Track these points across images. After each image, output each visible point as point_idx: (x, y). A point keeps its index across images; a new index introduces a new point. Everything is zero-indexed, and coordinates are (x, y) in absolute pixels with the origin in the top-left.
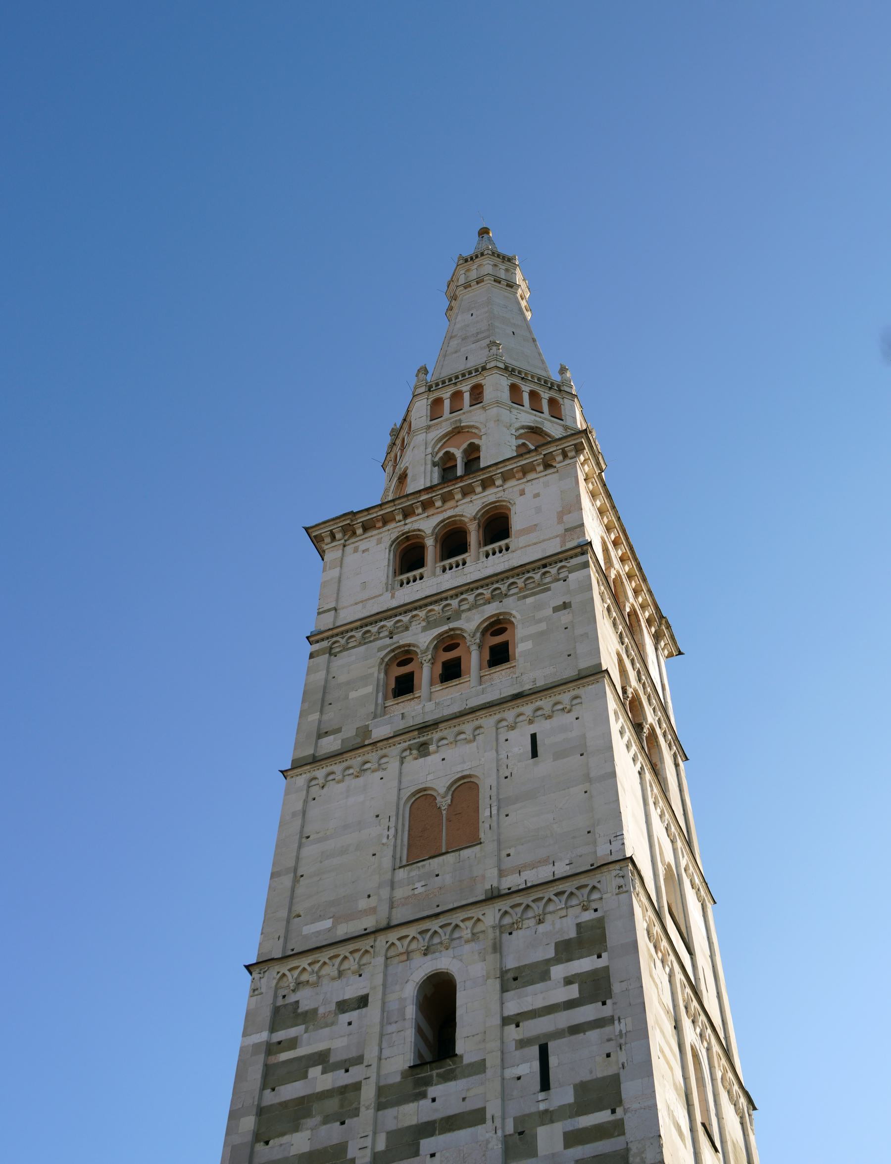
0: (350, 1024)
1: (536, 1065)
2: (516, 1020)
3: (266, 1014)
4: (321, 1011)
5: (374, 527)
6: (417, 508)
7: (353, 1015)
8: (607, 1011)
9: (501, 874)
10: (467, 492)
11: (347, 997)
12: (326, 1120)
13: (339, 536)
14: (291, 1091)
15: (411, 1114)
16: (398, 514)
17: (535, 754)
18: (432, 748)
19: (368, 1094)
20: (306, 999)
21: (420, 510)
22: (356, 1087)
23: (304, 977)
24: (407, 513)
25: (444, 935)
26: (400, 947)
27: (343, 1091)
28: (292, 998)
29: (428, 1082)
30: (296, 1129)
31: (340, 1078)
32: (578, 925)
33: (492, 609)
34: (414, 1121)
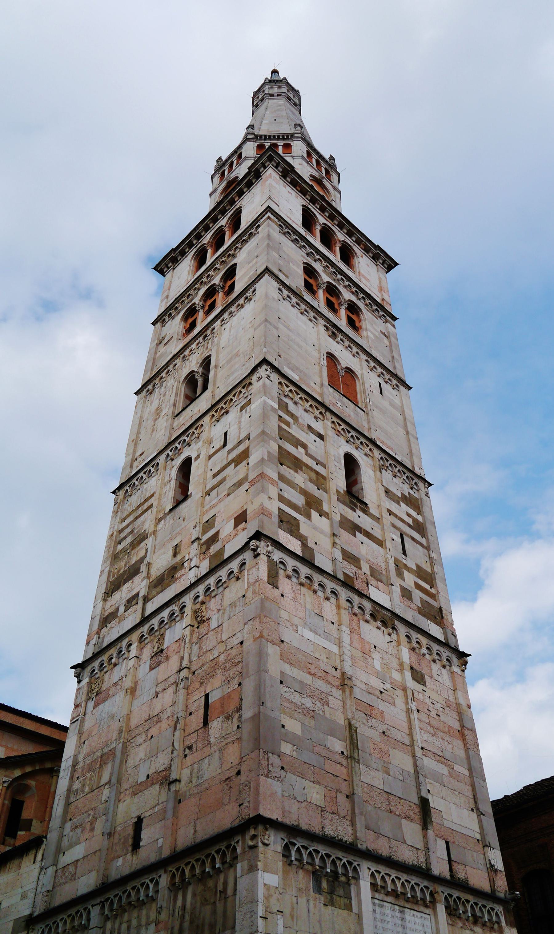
0: (315, 441)
2: (390, 513)
4: (300, 420)
5: (295, 187)
6: (318, 204)
7: (318, 439)
8: (423, 541)
10: (341, 226)
12: (311, 480)
13: (279, 168)
16: (309, 195)
17: (381, 393)
18: (338, 339)
20: (292, 407)
21: (318, 207)
23: (290, 394)
24: (313, 201)
25: (358, 442)
26: (340, 428)
27: (317, 473)
29: (356, 506)
30: (296, 472)
33: (354, 298)
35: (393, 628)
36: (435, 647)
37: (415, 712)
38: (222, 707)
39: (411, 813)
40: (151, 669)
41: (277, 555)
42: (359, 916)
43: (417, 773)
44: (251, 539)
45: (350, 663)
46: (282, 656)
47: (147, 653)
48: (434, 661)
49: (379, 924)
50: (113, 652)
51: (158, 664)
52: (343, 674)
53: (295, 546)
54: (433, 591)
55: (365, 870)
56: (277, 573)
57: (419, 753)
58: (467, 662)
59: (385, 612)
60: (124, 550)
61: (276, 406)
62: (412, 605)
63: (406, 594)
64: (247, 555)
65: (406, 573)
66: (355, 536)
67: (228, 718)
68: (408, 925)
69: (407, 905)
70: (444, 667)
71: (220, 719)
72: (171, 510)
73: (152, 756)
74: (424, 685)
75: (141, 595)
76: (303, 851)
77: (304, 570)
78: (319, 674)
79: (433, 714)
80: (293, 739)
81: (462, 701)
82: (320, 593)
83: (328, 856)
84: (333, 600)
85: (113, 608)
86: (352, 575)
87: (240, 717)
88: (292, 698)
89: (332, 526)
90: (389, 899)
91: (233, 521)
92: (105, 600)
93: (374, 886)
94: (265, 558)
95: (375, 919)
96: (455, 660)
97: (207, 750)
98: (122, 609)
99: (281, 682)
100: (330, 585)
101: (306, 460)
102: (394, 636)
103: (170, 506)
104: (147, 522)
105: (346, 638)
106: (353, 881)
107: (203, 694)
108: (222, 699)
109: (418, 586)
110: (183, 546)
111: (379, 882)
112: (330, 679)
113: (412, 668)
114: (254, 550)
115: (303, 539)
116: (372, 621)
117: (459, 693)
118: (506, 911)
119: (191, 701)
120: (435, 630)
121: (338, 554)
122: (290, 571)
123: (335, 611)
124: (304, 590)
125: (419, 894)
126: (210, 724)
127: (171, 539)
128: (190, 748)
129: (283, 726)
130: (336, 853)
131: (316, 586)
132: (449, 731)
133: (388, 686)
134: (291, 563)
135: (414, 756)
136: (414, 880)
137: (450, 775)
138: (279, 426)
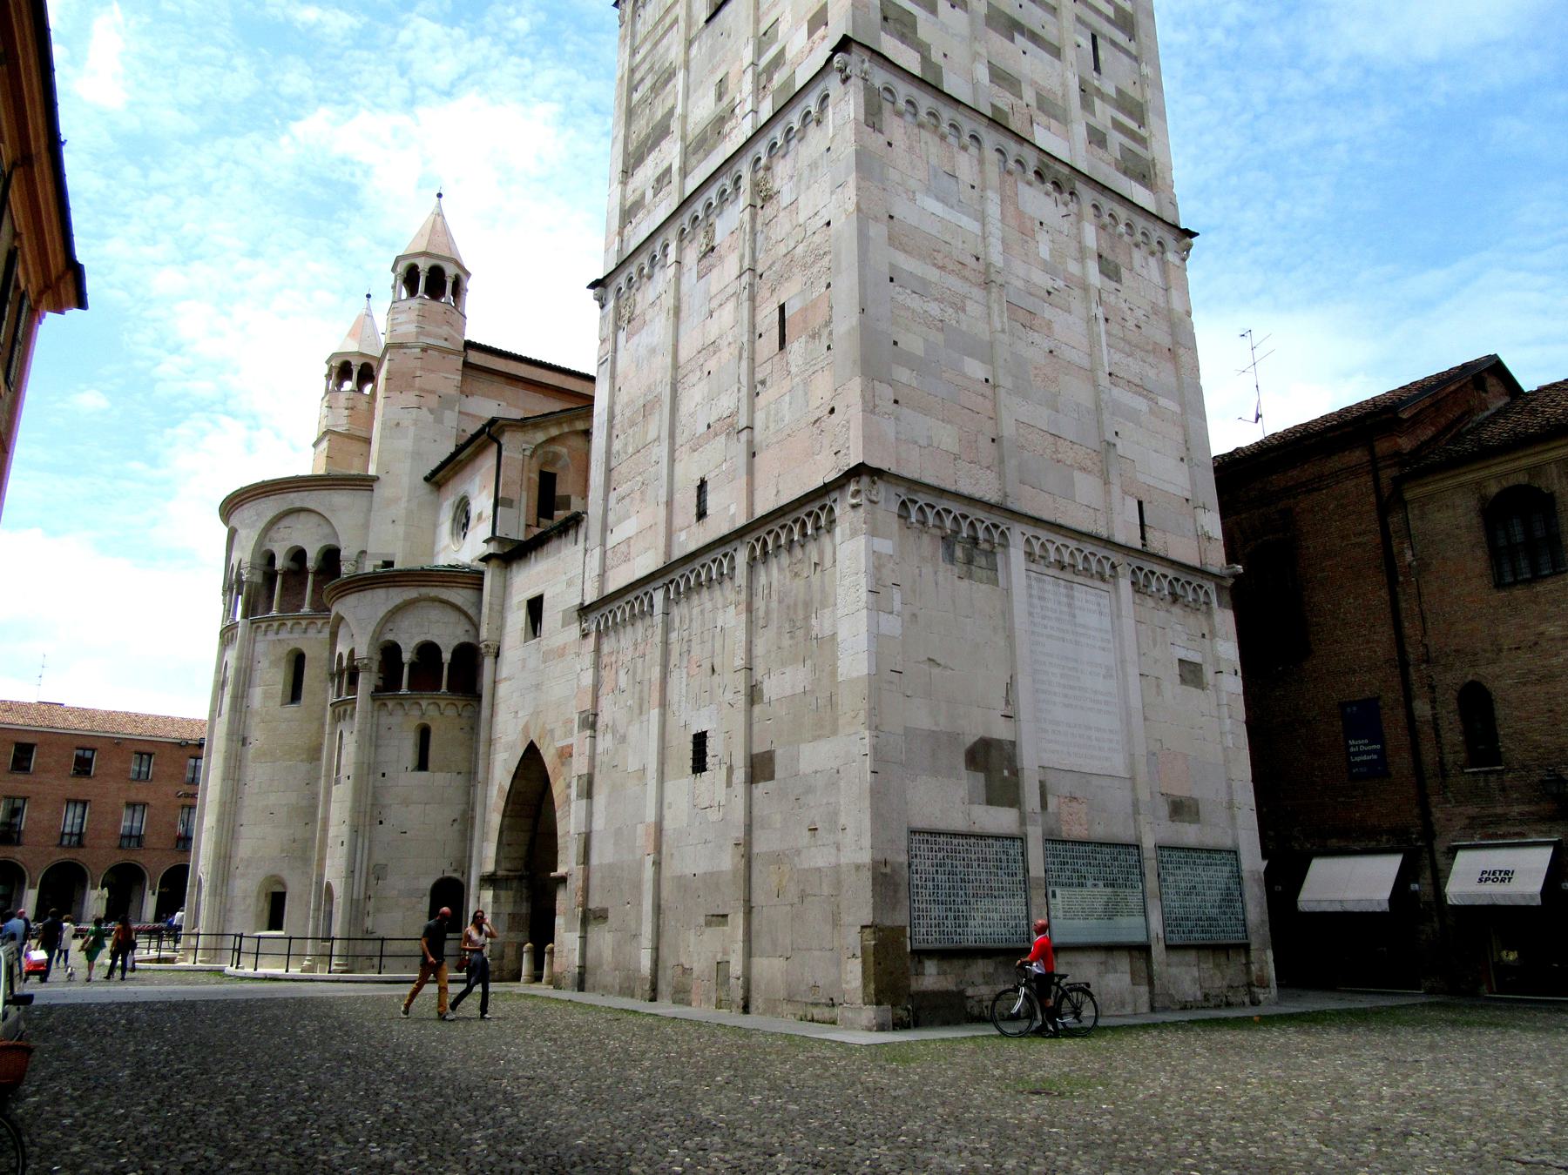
8: (1132, 47)
35: (1072, 194)
36: (1140, 223)
37: (1102, 321)
38: (805, 322)
39: (1089, 463)
40: (700, 277)
41: (880, 77)
42: (1008, 592)
43: (1098, 408)
44: (835, 50)
45: (1000, 248)
46: (892, 240)
47: (692, 255)
48: (1137, 245)
49: (1036, 601)
50: (644, 259)
51: (710, 269)
52: (988, 265)
53: (909, 60)
54: (1142, 132)
55: (1018, 534)
56: (880, 108)
58: (1190, 246)
59: (1058, 166)
60: (643, 100)
62: (1106, 156)
63: (1097, 138)
64: (833, 83)
65: (1097, 102)
66: (1012, 40)
67: (813, 337)
68: (1077, 603)
69: (1077, 579)
70: (1152, 254)
71: (803, 339)
72: (708, 21)
73: (711, 398)
74: (1119, 280)
75: (675, 168)
76: (927, 510)
77: (926, 101)
78: (950, 267)
79: (1131, 324)
80: (909, 361)
81: (1177, 305)
82: (952, 140)
83: (965, 517)
84: (973, 150)
85: (638, 193)
86: (1006, 109)
87: (831, 333)
88: (908, 302)
89: (972, 23)
90: (1051, 571)
91: (805, 26)
92: (624, 183)
93: (1029, 555)
94: (861, 83)
95: (1030, 596)
96: (1169, 239)
97: (787, 384)
98: (649, 193)
99: (892, 280)
100: (968, 125)
102: (1073, 207)
103: (704, 17)
104: (673, 48)
105: (993, 209)
106: (999, 550)
107: (776, 306)
108: (804, 310)
109: (1118, 126)
110: (732, 83)
111: (1037, 549)
112: (967, 273)
113: (1100, 256)
114: (841, 71)
115: (922, 49)
116: (1037, 183)
117: (1174, 293)
118: (1220, 588)
119: (759, 318)
120: (1141, 195)
121: (983, 74)
122: (901, 104)
123: (976, 168)
124: (925, 135)
125: (1094, 567)
126: (788, 346)
127: (712, 71)
128: (763, 383)
129: (895, 343)
130: (976, 513)
131: (945, 128)
132: (1155, 349)
133: (1060, 283)
134: (903, 90)
135: (1096, 385)
136: (1088, 548)
137: (1151, 411)
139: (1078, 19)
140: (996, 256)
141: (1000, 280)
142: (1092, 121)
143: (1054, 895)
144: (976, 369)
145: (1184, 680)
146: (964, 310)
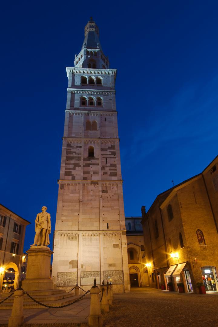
1: (105, 160)
3: (66, 145)
4: (74, 146)
7: (79, 148)
8: (115, 156)
9: (101, 136)
11: (78, 145)
12: (76, 160)
14: (71, 155)
15: (89, 162)
19: (82, 158)
20: (72, 145)
22: (81, 157)
27: (78, 157)
28: (69, 144)
30: (72, 160)
31: (78, 156)
32: (112, 146)
34: (89, 163)
45: (82, 196)
57: (101, 208)
61: (66, 147)
65: (106, 168)
66: (89, 167)
74: (107, 193)
79: (109, 198)
84: (79, 185)
101: (76, 155)
102: (98, 185)
115: (72, 175)
122: (67, 185)
133: (94, 197)
138: (67, 152)
139: (103, 158)
140: (81, 198)
141: (81, 201)
142: (104, 171)
143: (82, 279)
144: (77, 214)
145: (114, 247)
146: (75, 207)
